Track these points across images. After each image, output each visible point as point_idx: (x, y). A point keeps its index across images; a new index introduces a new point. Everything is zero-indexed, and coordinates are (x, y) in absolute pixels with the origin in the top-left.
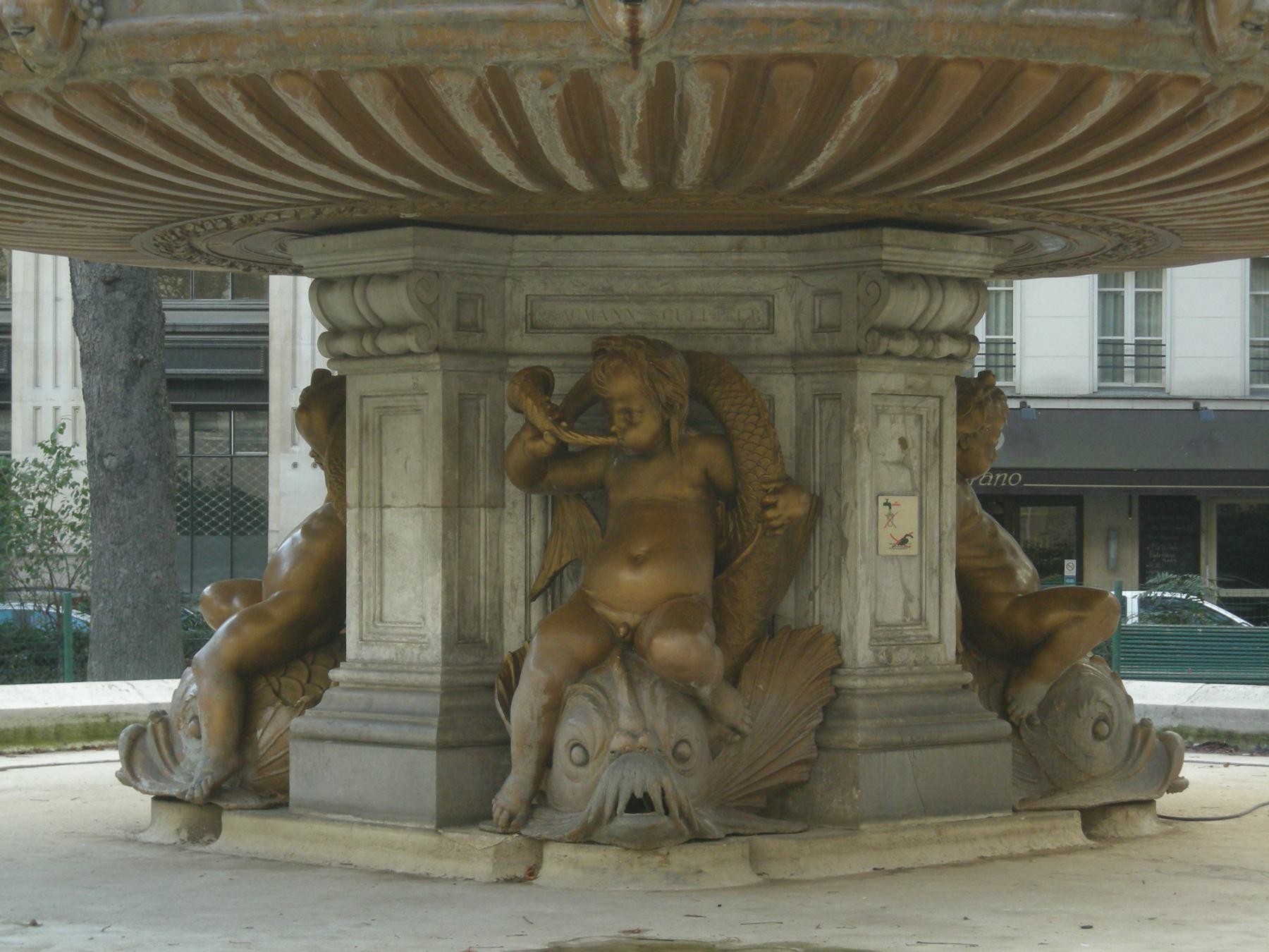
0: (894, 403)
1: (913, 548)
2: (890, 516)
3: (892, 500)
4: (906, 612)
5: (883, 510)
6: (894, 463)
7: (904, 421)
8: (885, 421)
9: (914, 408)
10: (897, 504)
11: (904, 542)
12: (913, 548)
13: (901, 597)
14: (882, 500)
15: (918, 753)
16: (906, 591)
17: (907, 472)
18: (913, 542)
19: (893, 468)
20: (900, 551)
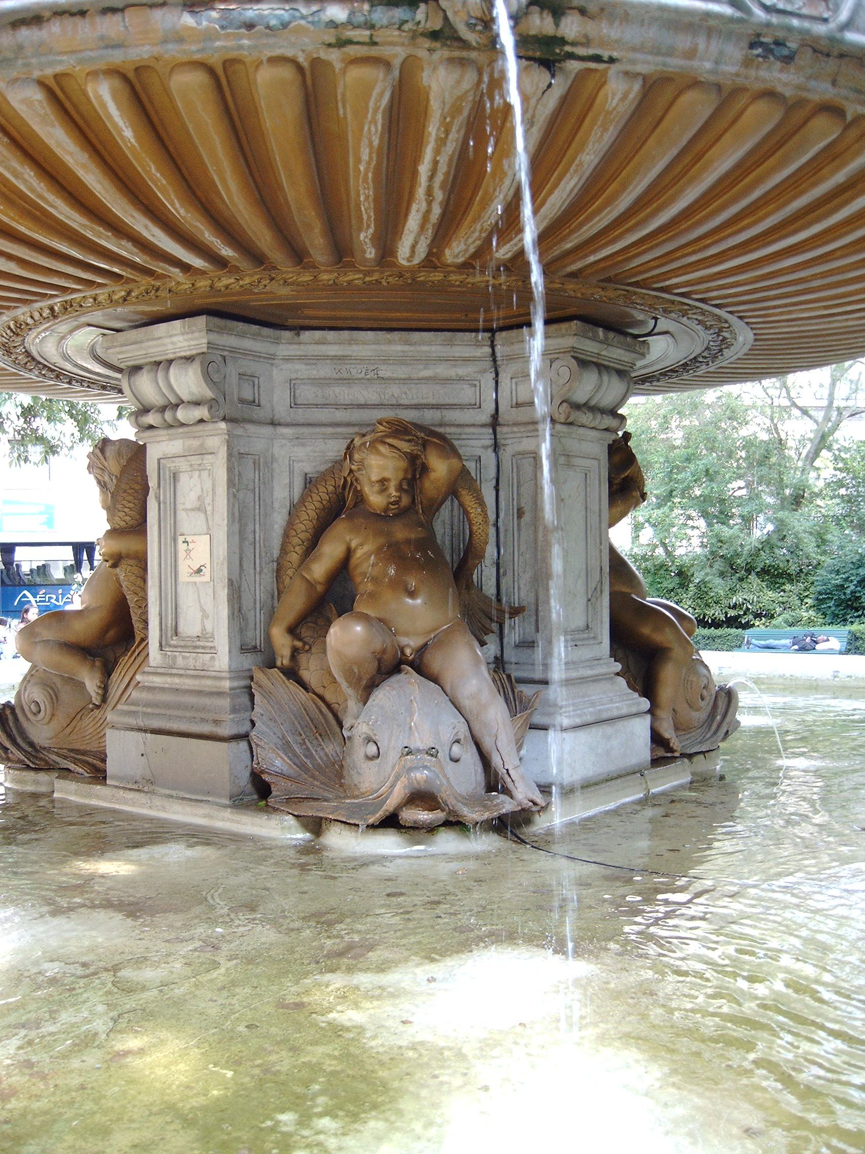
0: (182, 464)
1: (206, 576)
2: (188, 551)
3: (189, 539)
4: (204, 629)
5: (182, 547)
6: (192, 510)
7: (200, 476)
8: (183, 478)
9: (200, 465)
10: (193, 542)
11: (199, 571)
12: (206, 576)
13: (199, 615)
14: (181, 539)
15: (149, 735)
16: (203, 610)
17: (202, 516)
18: (206, 571)
19: (191, 514)
20: (197, 579)
